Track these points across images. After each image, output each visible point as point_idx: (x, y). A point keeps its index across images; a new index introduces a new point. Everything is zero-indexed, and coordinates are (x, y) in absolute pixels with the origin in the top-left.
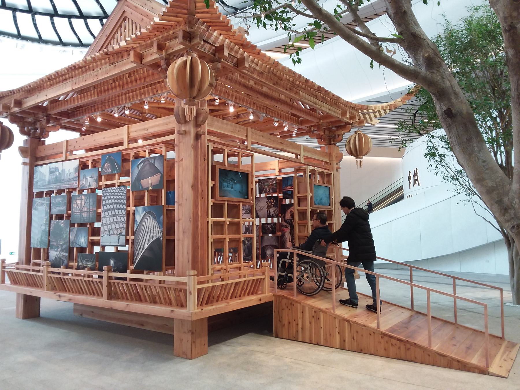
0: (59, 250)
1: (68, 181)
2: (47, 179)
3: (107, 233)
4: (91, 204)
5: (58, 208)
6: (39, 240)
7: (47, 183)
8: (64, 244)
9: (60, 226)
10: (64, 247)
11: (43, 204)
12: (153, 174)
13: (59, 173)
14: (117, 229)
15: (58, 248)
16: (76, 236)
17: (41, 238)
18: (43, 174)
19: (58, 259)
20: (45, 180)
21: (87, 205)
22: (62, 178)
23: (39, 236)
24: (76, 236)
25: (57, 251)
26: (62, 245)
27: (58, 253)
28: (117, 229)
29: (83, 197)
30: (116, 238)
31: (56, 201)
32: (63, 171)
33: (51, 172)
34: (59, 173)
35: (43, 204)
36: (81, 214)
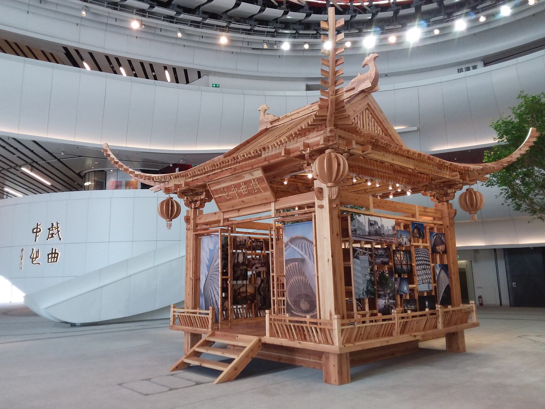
0: (387, 298)
1: (387, 236)
2: (367, 229)
3: (421, 282)
4: (408, 259)
5: (381, 259)
6: (365, 290)
7: (367, 234)
8: (391, 292)
9: (385, 276)
10: (391, 295)
11: (365, 253)
12: (442, 244)
13: (379, 227)
14: (427, 279)
15: (385, 296)
16: (400, 285)
17: (367, 287)
18: (362, 223)
19: (387, 307)
20: (365, 230)
21: (405, 259)
22: (382, 232)
23: (365, 286)
24: (400, 285)
25: (385, 300)
26: (389, 294)
27: (386, 301)
28: (427, 279)
29: (402, 253)
30: (427, 285)
31: (378, 253)
32: (382, 226)
33: (371, 224)
34: (379, 227)
35: (365, 253)
36: (402, 267)
